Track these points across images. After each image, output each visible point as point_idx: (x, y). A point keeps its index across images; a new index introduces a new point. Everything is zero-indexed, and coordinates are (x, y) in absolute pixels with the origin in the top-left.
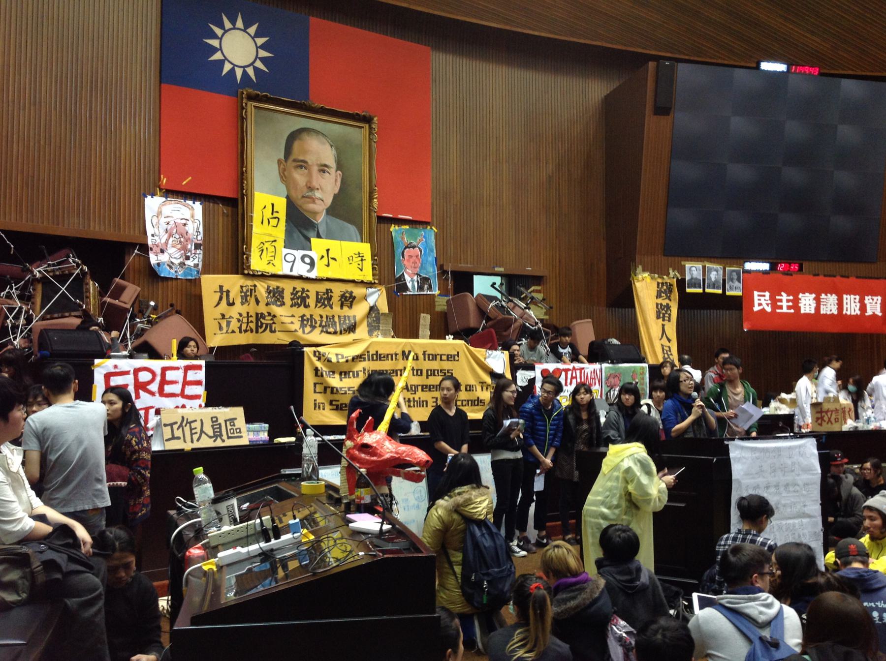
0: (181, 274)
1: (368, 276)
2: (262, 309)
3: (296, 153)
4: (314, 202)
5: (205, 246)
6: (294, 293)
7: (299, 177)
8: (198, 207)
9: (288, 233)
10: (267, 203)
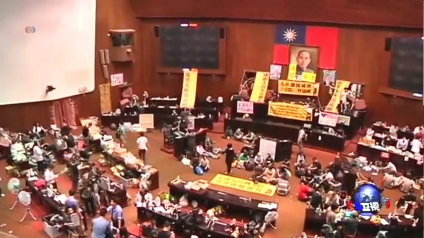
0: (276, 79)
1: (314, 81)
2: (290, 87)
3: (300, 55)
4: (303, 65)
5: (281, 74)
6: (297, 84)
7: (301, 60)
8: (280, 67)
9: (297, 71)
10: (293, 65)
